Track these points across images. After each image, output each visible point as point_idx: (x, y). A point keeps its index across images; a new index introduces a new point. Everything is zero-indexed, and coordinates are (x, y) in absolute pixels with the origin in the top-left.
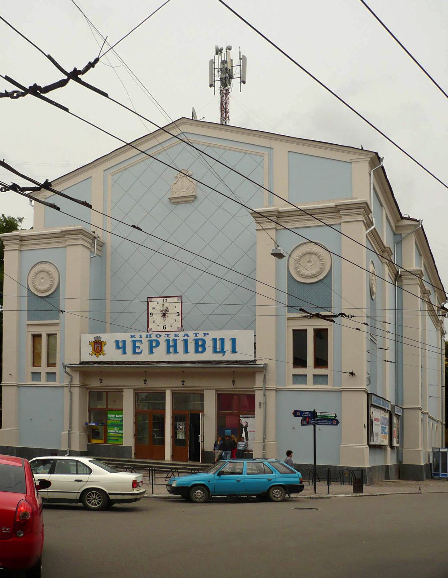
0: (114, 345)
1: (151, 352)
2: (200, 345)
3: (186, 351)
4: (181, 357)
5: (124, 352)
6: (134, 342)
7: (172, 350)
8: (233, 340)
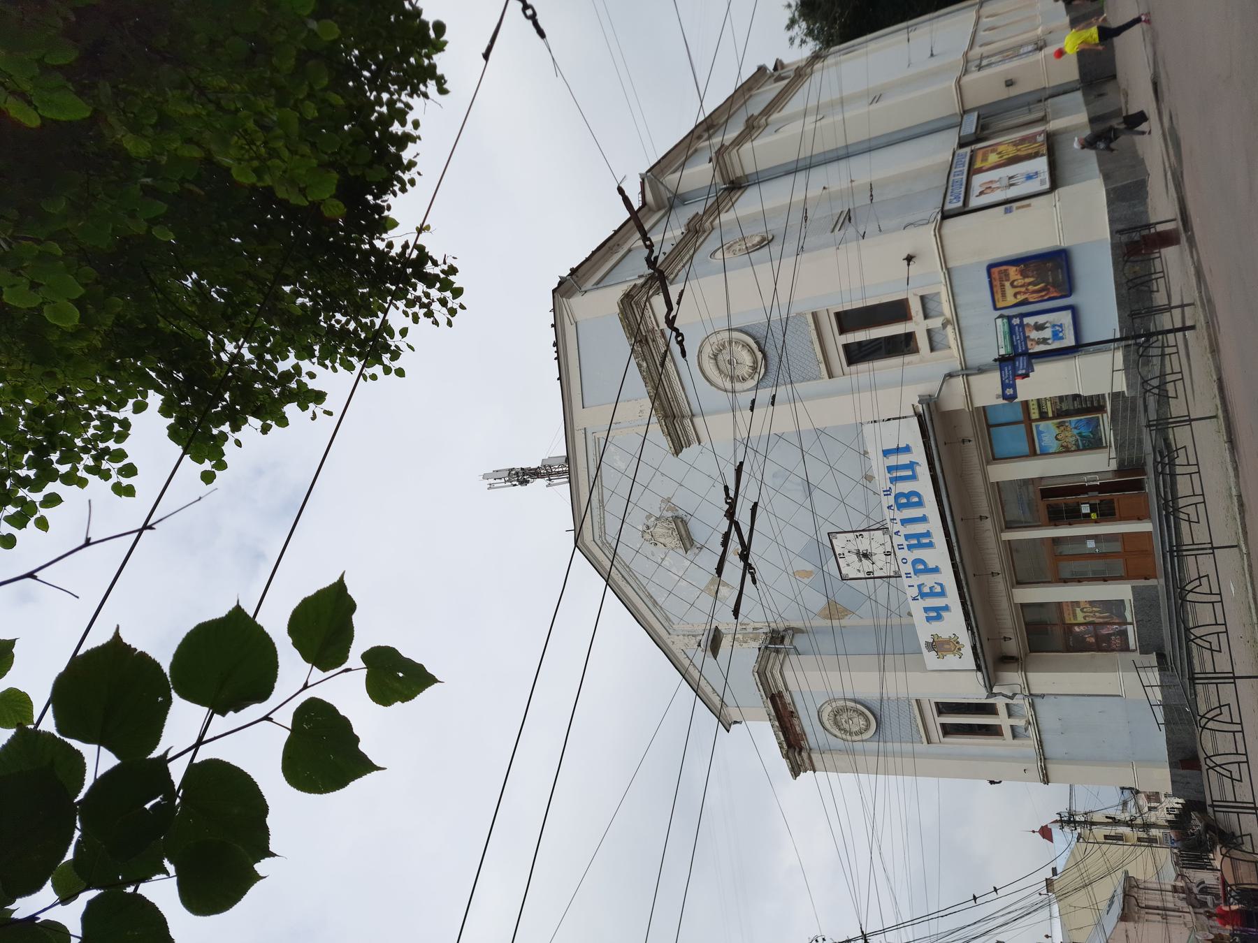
0: (935, 624)
1: (936, 570)
2: (909, 500)
3: (924, 519)
4: (934, 525)
5: (946, 608)
6: (923, 595)
7: (925, 541)
8: (886, 453)
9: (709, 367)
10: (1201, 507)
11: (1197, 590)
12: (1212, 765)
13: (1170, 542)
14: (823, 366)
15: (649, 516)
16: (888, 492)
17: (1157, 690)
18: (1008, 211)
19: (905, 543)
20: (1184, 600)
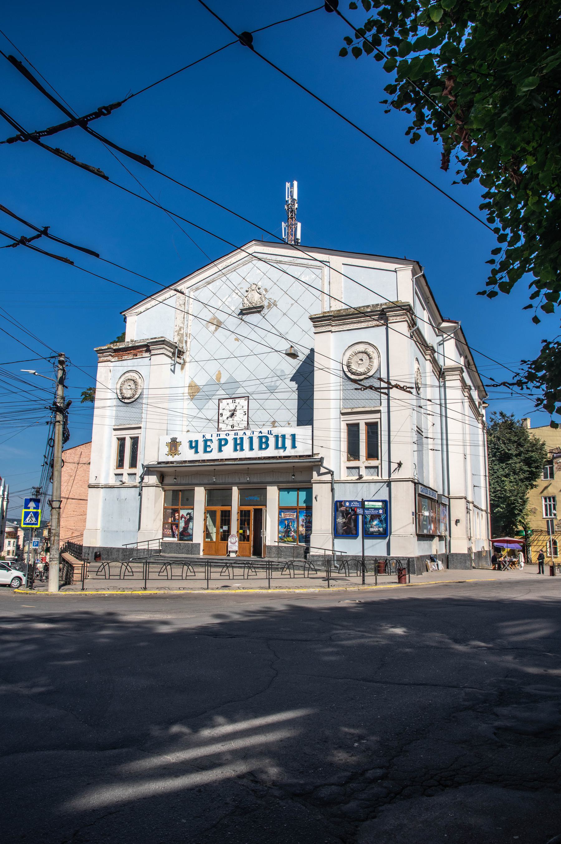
0: (188, 445)
1: (220, 450)
2: (263, 443)
3: (251, 449)
4: (246, 453)
5: (197, 452)
6: (206, 441)
7: (238, 447)
8: (293, 436)
9: (361, 348)
10: (228, 577)
11: (189, 570)
12: (104, 564)
13: (213, 562)
14: (349, 411)
15: (266, 290)
16: (270, 433)
17: (146, 547)
18: (413, 513)
19: (238, 437)
20: (185, 564)
